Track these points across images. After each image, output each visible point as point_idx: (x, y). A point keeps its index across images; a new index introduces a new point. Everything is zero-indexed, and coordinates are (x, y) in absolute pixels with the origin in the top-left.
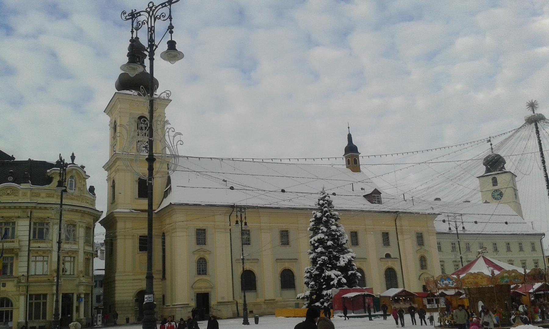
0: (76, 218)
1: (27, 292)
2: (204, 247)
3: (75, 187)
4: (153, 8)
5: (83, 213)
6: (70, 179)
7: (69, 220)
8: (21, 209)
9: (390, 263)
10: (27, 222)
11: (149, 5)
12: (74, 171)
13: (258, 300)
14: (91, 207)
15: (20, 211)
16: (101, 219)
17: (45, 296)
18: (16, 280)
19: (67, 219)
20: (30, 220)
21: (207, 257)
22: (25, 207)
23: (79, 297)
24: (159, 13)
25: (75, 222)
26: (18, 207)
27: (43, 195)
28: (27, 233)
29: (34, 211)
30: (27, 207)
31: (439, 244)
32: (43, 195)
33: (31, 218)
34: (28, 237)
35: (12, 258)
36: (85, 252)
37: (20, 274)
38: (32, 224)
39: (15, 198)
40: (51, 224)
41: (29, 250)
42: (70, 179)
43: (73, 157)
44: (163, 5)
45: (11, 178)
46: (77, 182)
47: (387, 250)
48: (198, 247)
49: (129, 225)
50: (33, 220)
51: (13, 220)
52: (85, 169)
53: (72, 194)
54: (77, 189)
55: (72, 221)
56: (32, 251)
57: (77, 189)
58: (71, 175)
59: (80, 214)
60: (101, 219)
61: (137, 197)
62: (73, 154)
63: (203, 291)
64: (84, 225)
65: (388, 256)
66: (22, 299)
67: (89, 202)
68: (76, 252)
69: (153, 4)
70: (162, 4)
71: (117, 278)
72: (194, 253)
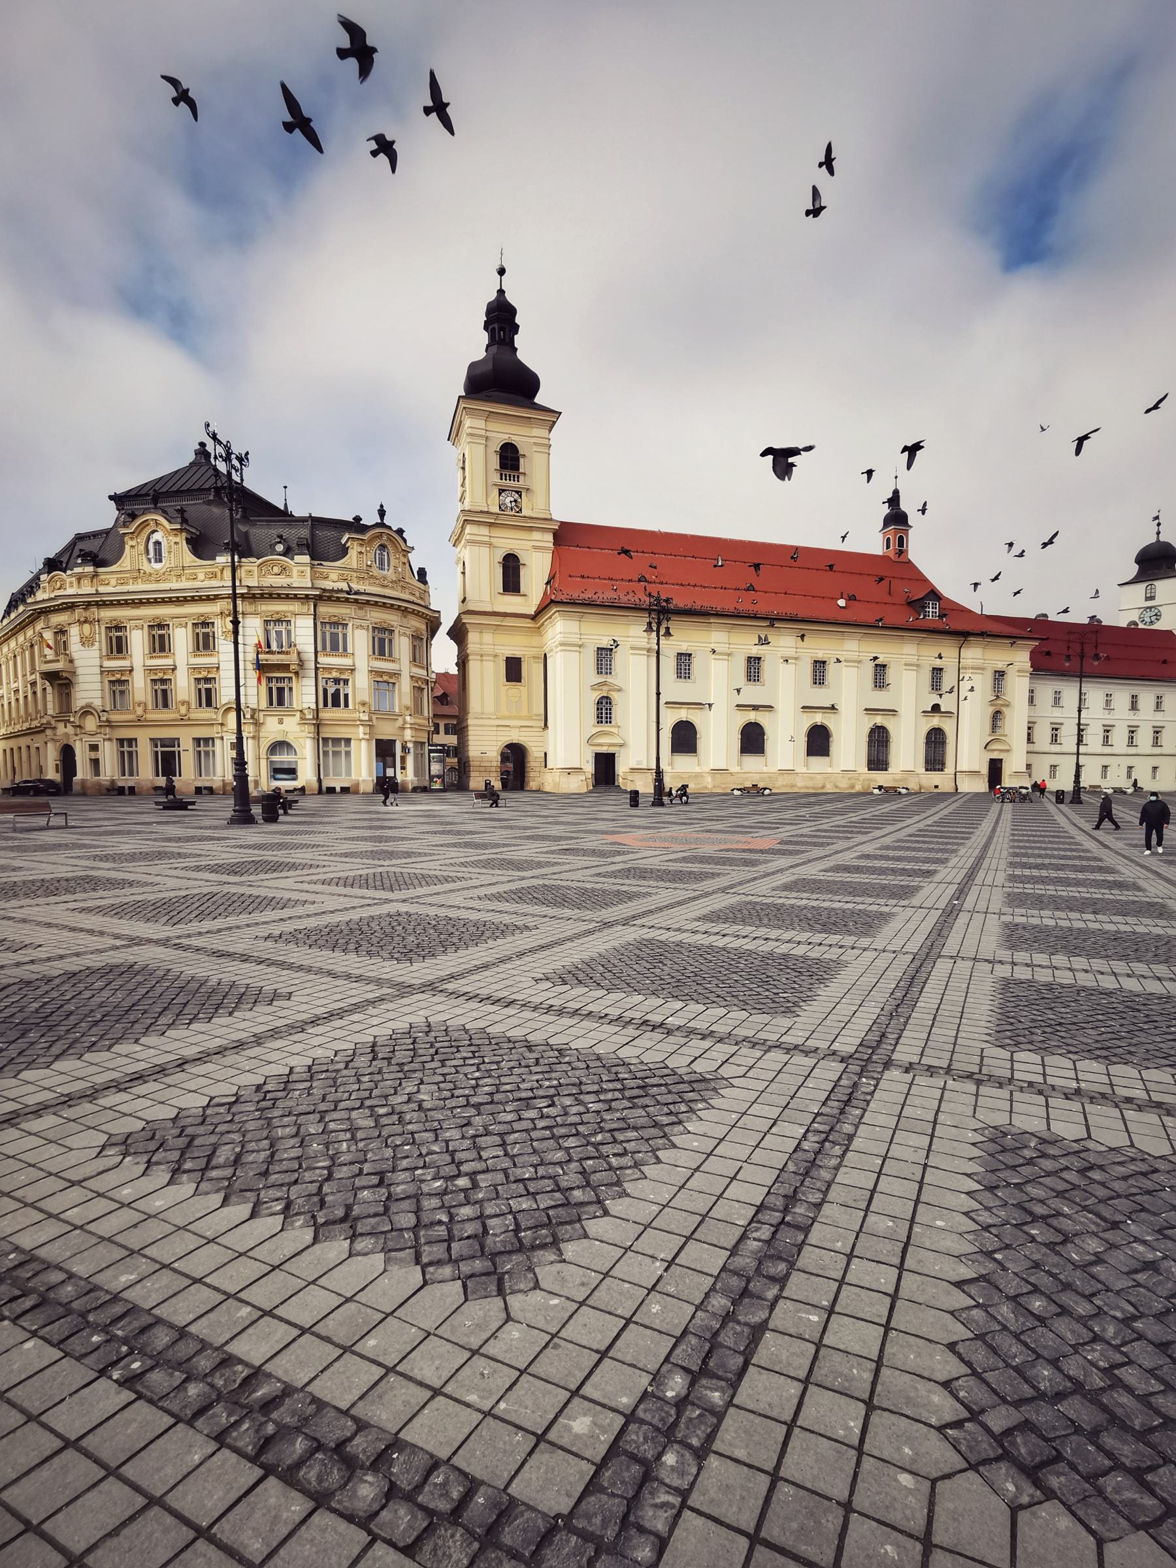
2: (609, 679)
5: (405, 611)
9: (936, 721)
10: (310, 622)
12: (385, 538)
18: (298, 714)
21: (614, 696)
30: (307, 597)
31: (1032, 691)
34: (313, 646)
35: (290, 679)
36: (412, 677)
37: (305, 706)
38: (319, 624)
41: (317, 669)
43: (382, 513)
45: (280, 548)
46: (392, 558)
47: (937, 700)
48: (601, 679)
49: (488, 637)
52: (405, 535)
53: (385, 578)
54: (392, 568)
57: (392, 568)
59: (399, 613)
62: (382, 506)
63: (604, 750)
64: (409, 632)
65: (936, 708)
67: (417, 594)
68: (396, 675)
71: (470, 722)
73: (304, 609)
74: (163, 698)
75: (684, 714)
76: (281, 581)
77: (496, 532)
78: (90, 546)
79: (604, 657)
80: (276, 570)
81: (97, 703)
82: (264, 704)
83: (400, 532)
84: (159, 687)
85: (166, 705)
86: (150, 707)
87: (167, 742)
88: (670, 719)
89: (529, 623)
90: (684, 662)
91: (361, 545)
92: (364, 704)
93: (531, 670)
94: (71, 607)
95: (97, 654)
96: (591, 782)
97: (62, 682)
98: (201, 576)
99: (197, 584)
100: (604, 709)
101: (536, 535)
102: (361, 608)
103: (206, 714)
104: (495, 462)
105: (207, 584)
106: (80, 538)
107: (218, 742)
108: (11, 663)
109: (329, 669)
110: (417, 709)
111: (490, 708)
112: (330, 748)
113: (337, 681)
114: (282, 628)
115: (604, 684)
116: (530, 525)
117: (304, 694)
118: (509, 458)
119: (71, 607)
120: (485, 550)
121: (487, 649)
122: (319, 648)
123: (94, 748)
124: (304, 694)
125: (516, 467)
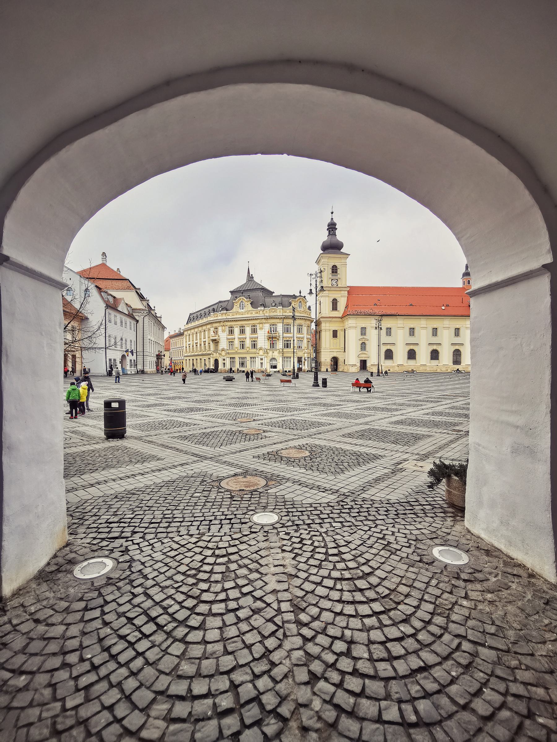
0: (302, 322)
2: (365, 337)
13: (393, 365)
17: (290, 357)
21: (366, 342)
23: (305, 360)
27: (288, 312)
32: (288, 312)
43: (300, 292)
48: (362, 337)
49: (328, 325)
66: (281, 358)
68: (303, 338)
72: (359, 340)
74: (243, 346)
75: (389, 347)
76: (275, 314)
77: (330, 292)
78: (224, 305)
79: (363, 331)
81: (225, 348)
82: (269, 348)
83: (305, 297)
84: (242, 343)
85: (243, 348)
87: (243, 358)
88: (384, 349)
89: (340, 320)
90: (389, 331)
93: (340, 334)
94: (220, 322)
96: (359, 369)
97: (216, 342)
98: (254, 313)
100: (363, 346)
101: (342, 292)
103: (254, 350)
104: (330, 271)
105: (255, 315)
106: (220, 302)
108: (195, 335)
109: (286, 338)
110: (308, 348)
111: (328, 346)
112: (286, 359)
113: (287, 341)
114: (275, 327)
115: (363, 338)
116: (341, 289)
117: (280, 345)
118: (334, 269)
119: (220, 322)
120: (327, 298)
121: (327, 328)
123: (224, 360)
124: (280, 345)
125: (336, 272)
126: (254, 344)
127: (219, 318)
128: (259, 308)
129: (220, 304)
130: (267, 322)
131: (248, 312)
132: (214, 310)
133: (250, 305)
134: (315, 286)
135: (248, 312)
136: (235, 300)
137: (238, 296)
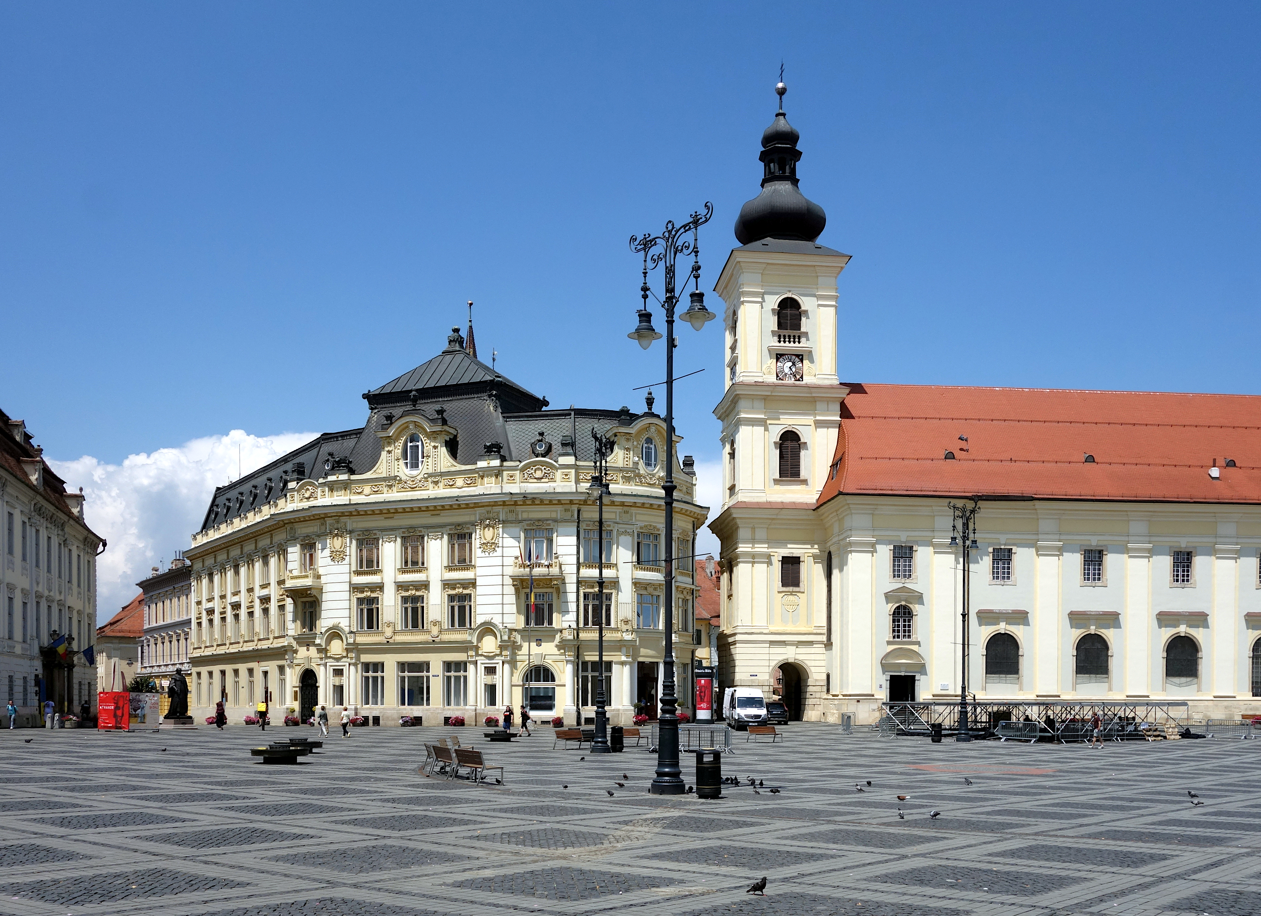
1: (578, 657)
3: (655, 460)
4: (673, 233)
6: (645, 445)
7: (646, 526)
8: (562, 504)
11: (667, 228)
12: (653, 429)
14: (687, 498)
15: (559, 508)
16: (708, 522)
19: (642, 524)
20: (578, 527)
22: (568, 502)
24: (680, 243)
25: (658, 530)
26: (556, 502)
28: (574, 550)
29: (583, 508)
30: (571, 502)
33: (578, 523)
34: (575, 558)
39: (552, 484)
40: (615, 532)
41: (579, 583)
42: (645, 445)
44: (686, 227)
50: (583, 526)
51: (549, 525)
55: (652, 528)
56: (583, 584)
58: (647, 436)
60: (708, 522)
61: (777, 476)
69: (673, 225)
70: (684, 226)
73: (568, 516)
80: (539, 474)
86: (399, 627)
91: (628, 440)
92: (626, 622)
95: (346, 569)
99: (454, 492)
102: (626, 512)
107: (471, 668)
122: (581, 560)
126: (462, 609)
127: (320, 502)
128: (481, 464)
129: (327, 448)
130: (511, 517)
131: (436, 477)
132: (300, 472)
133: (443, 451)
134: (663, 297)
135: (436, 477)
136: (384, 428)
137: (397, 411)
